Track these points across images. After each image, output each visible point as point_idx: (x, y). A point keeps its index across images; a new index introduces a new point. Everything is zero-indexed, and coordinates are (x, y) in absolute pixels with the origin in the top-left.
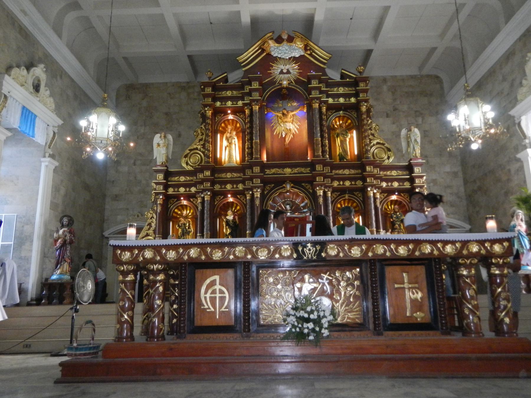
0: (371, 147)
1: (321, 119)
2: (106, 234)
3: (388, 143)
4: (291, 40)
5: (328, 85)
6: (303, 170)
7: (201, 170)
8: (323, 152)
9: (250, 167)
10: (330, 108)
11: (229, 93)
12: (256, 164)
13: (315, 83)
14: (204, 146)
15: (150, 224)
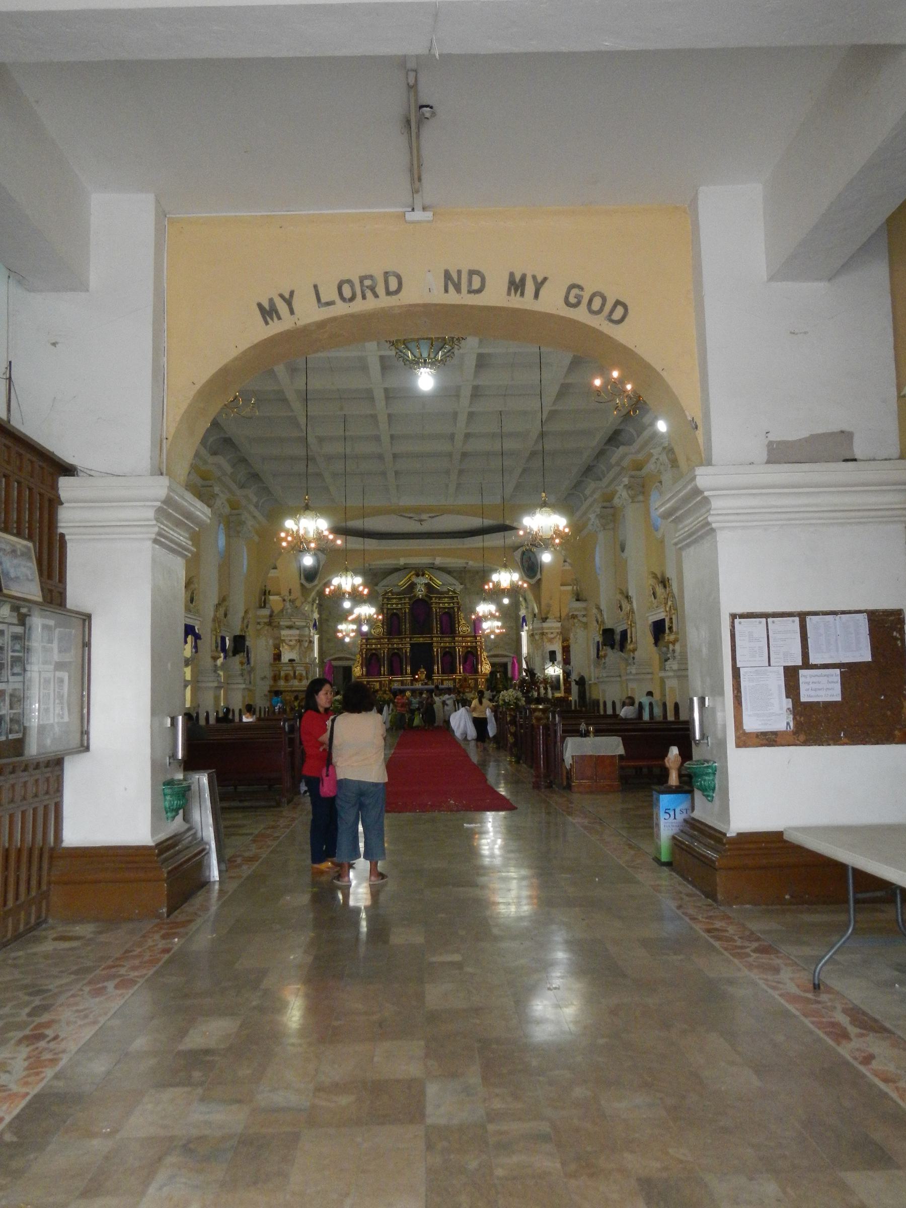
0: (459, 626)
1: (436, 616)
2: (325, 661)
3: (468, 623)
4: (423, 575)
5: (440, 598)
6: (428, 639)
7: (383, 638)
8: (437, 630)
9: (405, 638)
10: (440, 608)
11: (394, 601)
12: (407, 637)
13: (434, 599)
14: (382, 624)
15: (359, 662)
